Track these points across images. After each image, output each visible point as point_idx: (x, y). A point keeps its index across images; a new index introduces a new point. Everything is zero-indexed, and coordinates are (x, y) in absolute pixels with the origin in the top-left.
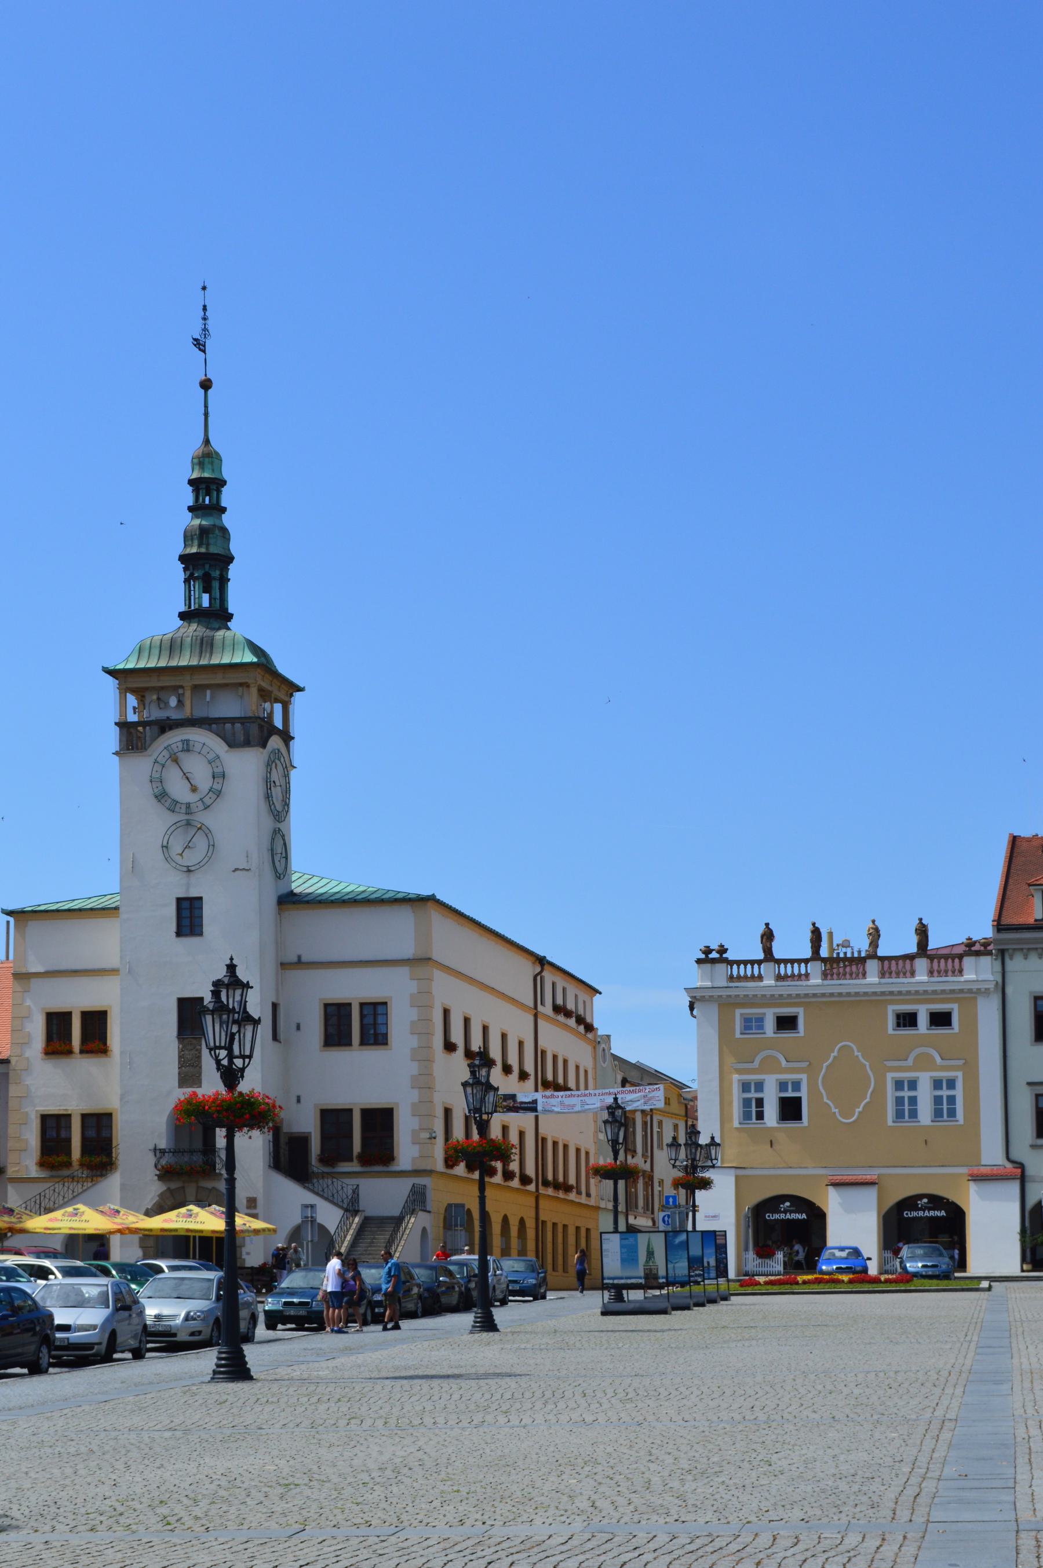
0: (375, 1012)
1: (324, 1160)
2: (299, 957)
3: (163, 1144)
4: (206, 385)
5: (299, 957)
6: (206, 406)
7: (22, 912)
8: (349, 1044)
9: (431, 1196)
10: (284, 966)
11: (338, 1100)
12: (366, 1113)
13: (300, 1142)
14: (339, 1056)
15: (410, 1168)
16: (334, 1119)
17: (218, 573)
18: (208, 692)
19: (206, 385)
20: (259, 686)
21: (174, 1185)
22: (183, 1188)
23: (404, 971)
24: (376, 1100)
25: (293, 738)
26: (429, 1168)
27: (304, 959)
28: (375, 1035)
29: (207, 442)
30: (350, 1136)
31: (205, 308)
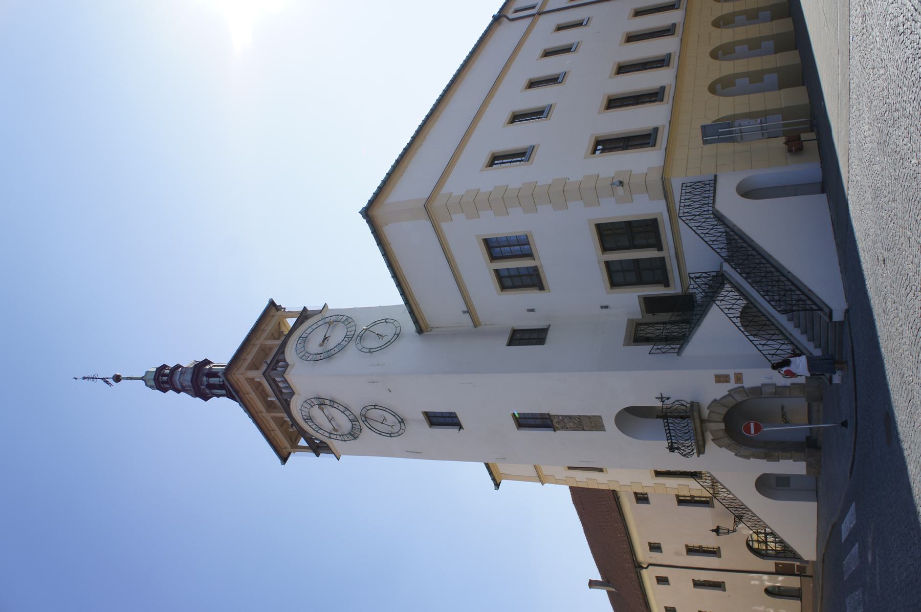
0: (495, 248)
1: (667, 285)
2: (464, 312)
3: (665, 444)
4: (117, 378)
5: (464, 312)
6: (127, 378)
7: (494, 479)
8: (535, 269)
9: (694, 176)
10: (476, 324)
11: (600, 276)
12: (605, 249)
13: (650, 304)
14: (549, 275)
15: (664, 202)
16: (618, 276)
17: (205, 379)
18: (269, 399)
19: (117, 378)
20: (246, 369)
21: (709, 436)
22: (711, 432)
23: (445, 226)
24: (591, 242)
25: (305, 308)
26: (661, 183)
27: (465, 309)
28: (520, 246)
29: (142, 379)
30: (636, 262)
31: (84, 378)
